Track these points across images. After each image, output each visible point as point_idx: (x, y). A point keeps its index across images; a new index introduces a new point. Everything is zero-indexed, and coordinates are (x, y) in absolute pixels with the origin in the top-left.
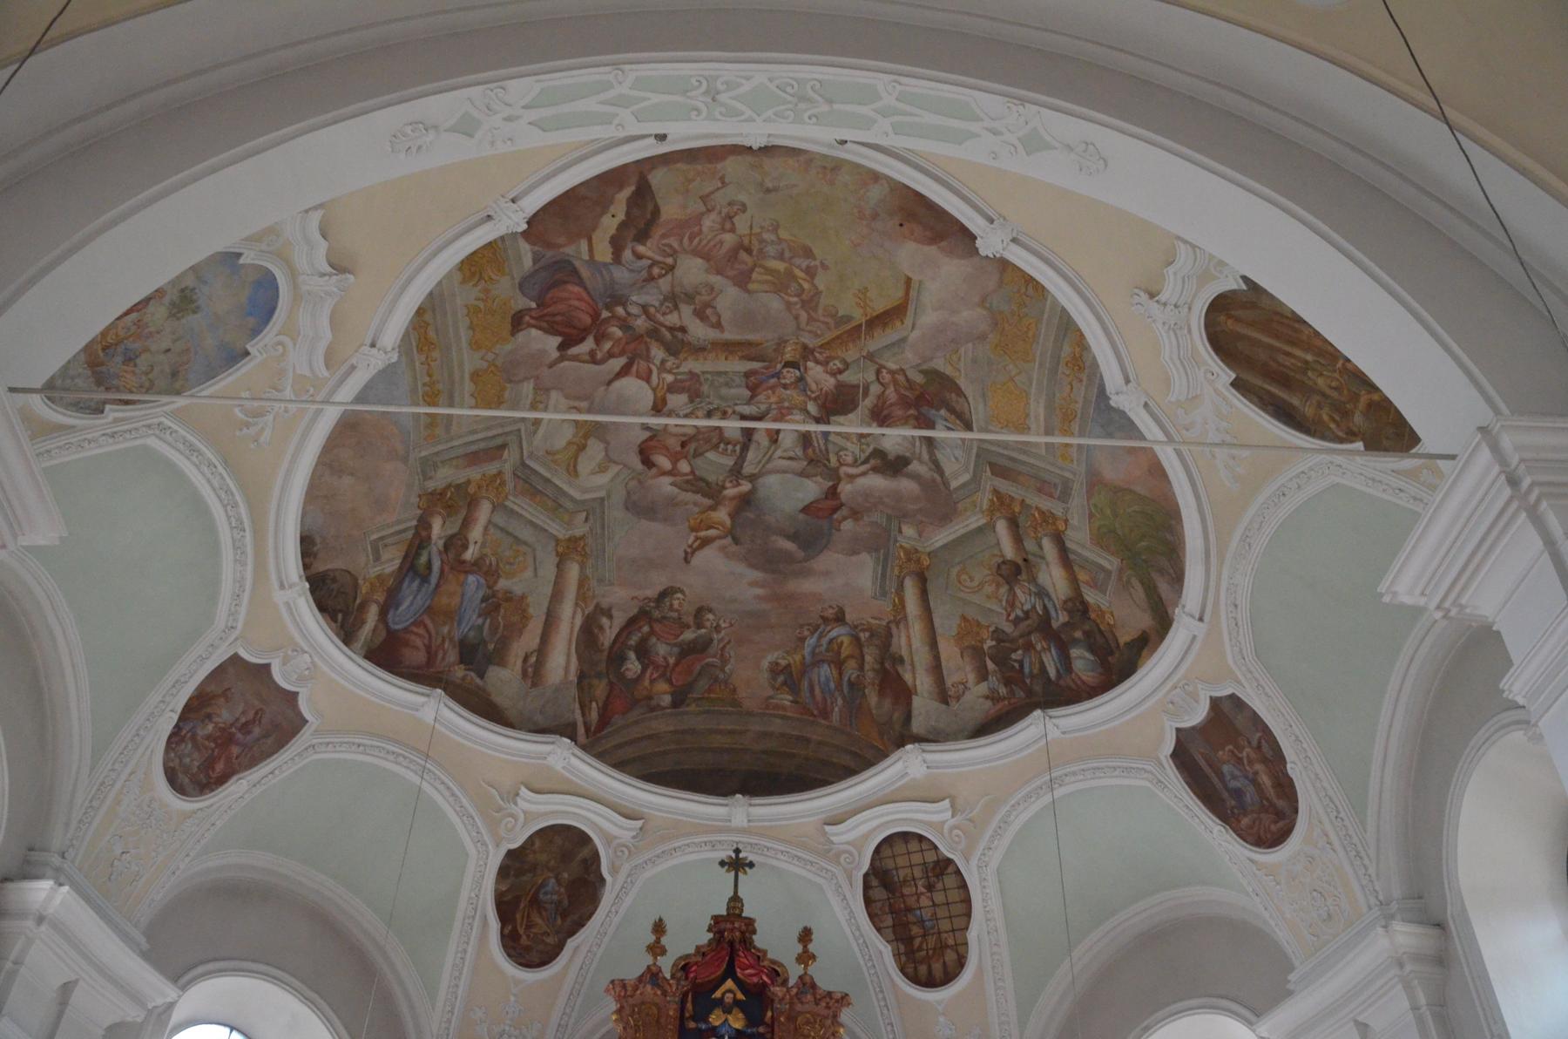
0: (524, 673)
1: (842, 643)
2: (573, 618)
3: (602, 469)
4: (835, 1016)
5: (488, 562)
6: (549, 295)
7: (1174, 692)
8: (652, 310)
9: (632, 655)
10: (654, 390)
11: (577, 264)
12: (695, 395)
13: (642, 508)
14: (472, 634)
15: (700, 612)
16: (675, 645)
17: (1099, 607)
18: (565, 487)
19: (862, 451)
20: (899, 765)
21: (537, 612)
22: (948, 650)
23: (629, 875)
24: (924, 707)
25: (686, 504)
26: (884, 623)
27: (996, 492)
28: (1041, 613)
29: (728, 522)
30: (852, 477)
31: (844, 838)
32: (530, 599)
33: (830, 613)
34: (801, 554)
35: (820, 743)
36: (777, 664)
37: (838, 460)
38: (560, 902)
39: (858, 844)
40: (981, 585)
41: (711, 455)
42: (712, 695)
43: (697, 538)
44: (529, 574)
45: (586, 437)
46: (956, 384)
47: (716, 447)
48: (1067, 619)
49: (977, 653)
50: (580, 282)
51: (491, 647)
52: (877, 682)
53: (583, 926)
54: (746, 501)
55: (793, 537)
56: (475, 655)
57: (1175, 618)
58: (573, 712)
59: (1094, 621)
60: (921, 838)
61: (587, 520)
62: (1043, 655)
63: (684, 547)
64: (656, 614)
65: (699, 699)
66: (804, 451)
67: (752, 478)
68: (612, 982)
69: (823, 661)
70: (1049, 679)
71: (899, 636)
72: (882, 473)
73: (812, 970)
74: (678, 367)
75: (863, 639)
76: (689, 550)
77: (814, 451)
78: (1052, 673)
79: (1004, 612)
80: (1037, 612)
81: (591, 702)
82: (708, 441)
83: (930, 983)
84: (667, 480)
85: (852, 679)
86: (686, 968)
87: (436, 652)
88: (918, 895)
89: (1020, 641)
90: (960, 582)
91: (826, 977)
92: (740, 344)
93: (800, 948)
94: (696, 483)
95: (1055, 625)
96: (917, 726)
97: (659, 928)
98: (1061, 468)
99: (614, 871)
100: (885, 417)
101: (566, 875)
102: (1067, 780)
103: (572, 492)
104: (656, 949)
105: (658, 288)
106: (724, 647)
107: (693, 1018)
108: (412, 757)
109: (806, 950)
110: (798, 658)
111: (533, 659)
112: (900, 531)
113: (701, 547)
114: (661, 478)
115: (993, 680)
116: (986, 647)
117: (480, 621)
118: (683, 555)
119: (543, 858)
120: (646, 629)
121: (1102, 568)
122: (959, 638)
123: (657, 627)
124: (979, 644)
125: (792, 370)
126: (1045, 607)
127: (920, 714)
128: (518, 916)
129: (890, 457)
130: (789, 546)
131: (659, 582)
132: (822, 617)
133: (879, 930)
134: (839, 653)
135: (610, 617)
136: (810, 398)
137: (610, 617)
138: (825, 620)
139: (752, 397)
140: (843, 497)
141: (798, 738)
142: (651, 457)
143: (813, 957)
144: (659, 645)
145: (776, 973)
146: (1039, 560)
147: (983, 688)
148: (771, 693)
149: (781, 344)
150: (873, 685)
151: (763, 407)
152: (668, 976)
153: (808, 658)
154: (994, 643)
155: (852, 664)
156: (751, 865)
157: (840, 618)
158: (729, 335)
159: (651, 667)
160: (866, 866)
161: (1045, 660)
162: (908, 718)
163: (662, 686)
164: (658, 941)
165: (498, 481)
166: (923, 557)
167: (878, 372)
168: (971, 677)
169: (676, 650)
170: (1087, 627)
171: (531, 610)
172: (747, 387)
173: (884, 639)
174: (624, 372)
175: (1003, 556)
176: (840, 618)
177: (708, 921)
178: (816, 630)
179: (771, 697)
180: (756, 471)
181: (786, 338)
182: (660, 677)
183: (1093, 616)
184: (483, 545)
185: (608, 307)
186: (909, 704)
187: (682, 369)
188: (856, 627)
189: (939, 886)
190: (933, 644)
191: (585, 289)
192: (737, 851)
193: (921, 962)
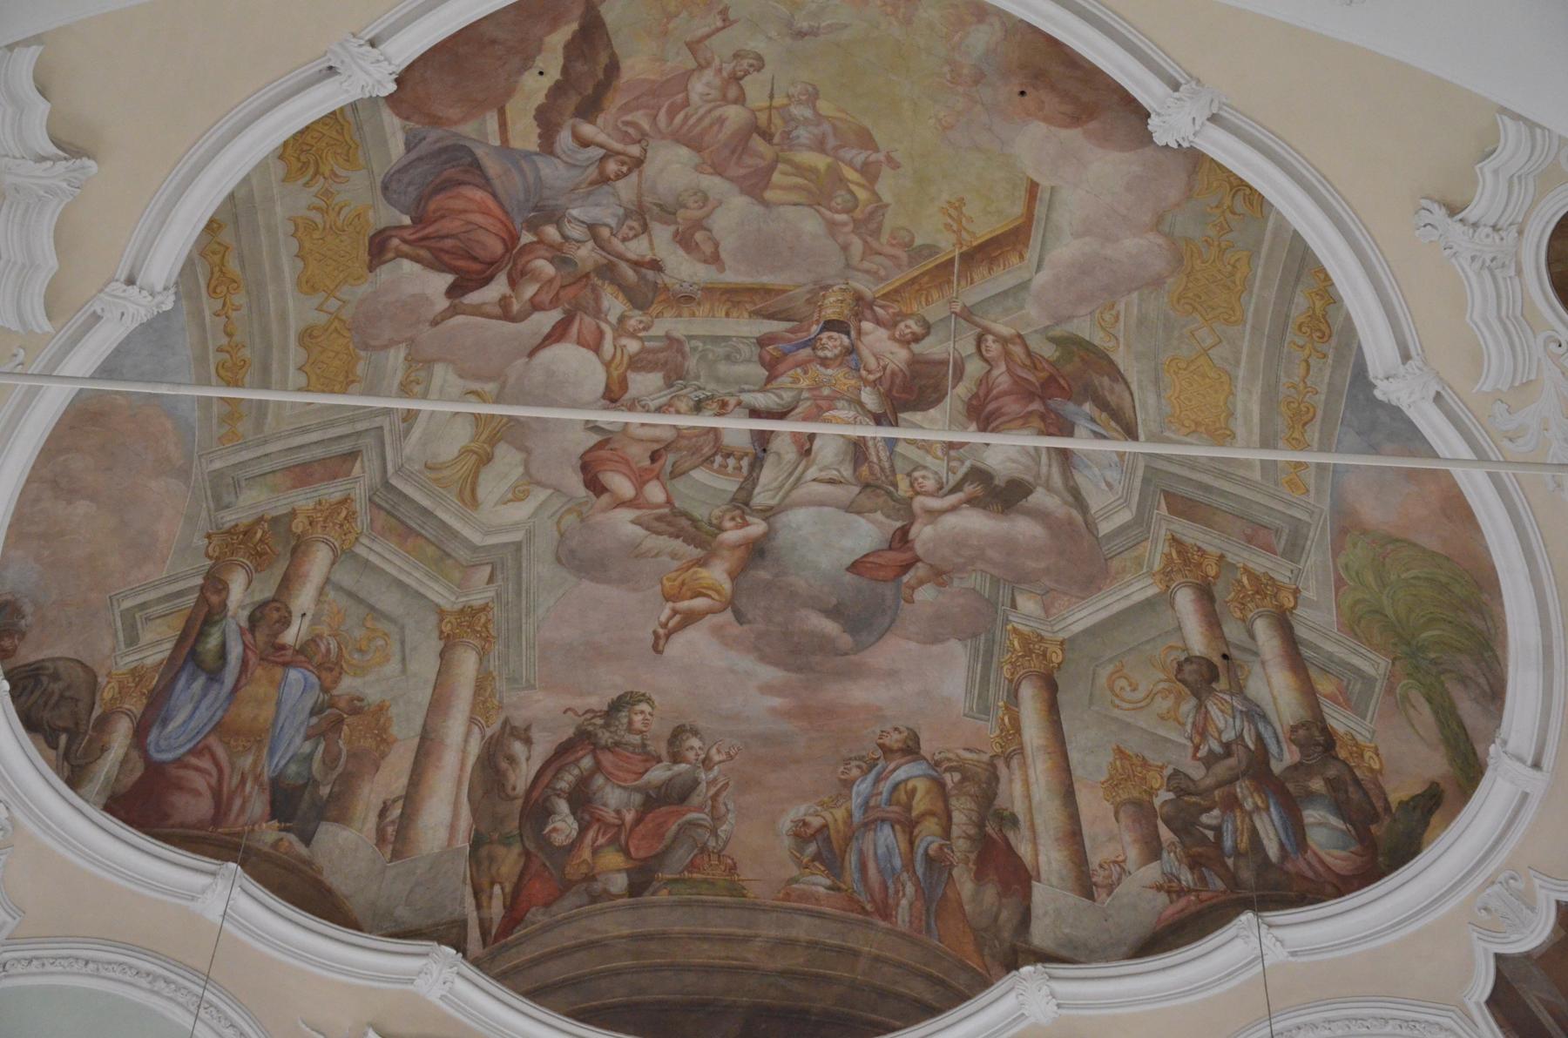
1: (914, 791)
2: (466, 741)
3: (518, 495)
5: (323, 648)
6: (432, 206)
7: (1488, 891)
8: (605, 232)
9: (563, 806)
10: (607, 365)
11: (480, 152)
12: (675, 375)
14: (293, 768)
15: (678, 734)
16: (637, 789)
17: (1354, 738)
18: (456, 525)
19: (951, 470)
20: (1009, 1002)
21: (405, 730)
22: (1093, 806)
25: (657, 555)
26: (985, 758)
27: (1175, 541)
28: (1252, 747)
29: (727, 586)
30: (933, 514)
32: (393, 711)
33: (893, 740)
34: (846, 640)
35: (877, 959)
36: (805, 824)
37: (912, 485)
40: (1151, 696)
41: (700, 475)
42: (695, 875)
43: (675, 612)
44: (393, 667)
45: (493, 441)
46: (1112, 363)
47: (709, 460)
48: (1297, 757)
49: (1143, 812)
50: (486, 183)
51: (325, 791)
52: (973, 856)
54: (757, 551)
55: (834, 613)
57: (1491, 762)
58: (462, 902)
59: (1344, 762)
61: (491, 580)
62: (1256, 818)
63: (654, 625)
64: (605, 737)
65: (676, 881)
66: (855, 470)
67: (768, 513)
69: (883, 820)
70: (1266, 857)
71: (1011, 781)
72: (984, 508)
74: (646, 329)
75: (950, 784)
76: (661, 631)
77: (871, 469)
78: (1273, 850)
79: (1189, 744)
80: (1247, 747)
81: (492, 884)
82: (695, 450)
84: (626, 515)
85: (931, 852)
87: (231, 799)
89: (1216, 792)
90: (1112, 690)
92: (751, 291)
94: (675, 522)
95: (1277, 767)
96: (1040, 935)
98: (1290, 504)
100: (992, 413)
103: (466, 532)
105: (616, 194)
106: (717, 794)
108: (180, 980)
110: (840, 814)
111: (396, 812)
112: (1014, 606)
113: (682, 626)
114: (617, 510)
115: (1171, 861)
116: (1157, 802)
117: (307, 747)
118: (650, 639)
120: (587, 763)
121: (1358, 672)
123: (607, 759)
124: (1146, 797)
125: (835, 335)
126: (1259, 738)
127: (1046, 913)
129: (996, 482)
130: (830, 627)
131: (608, 684)
132: (882, 746)
134: (909, 808)
135: (528, 741)
136: (866, 382)
137: (528, 741)
138: (887, 751)
139: (770, 380)
140: (919, 549)
141: (841, 950)
142: (601, 476)
144: (608, 789)
146: (1253, 658)
147: (1152, 872)
150: (967, 862)
151: (788, 396)
153: (858, 817)
154: (1171, 796)
155: (930, 826)
157: (911, 749)
158: (731, 277)
159: (596, 827)
161: (1259, 825)
163: (613, 859)
165: (343, 514)
166: (1051, 648)
167: (980, 341)
168: (1133, 853)
169: (637, 798)
170: (1332, 772)
171: (394, 730)
172: (763, 364)
173: (986, 787)
174: (557, 334)
175: (1186, 649)
176: (911, 749)
178: (870, 770)
179: (794, 880)
180: (772, 502)
181: (830, 282)
182: (611, 842)
183: (1342, 754)
184: (316, 620)
185: (533, 226)
187: (652, 332)
188: (937, 764)
190: (1068, 795)
191: (494, 195)
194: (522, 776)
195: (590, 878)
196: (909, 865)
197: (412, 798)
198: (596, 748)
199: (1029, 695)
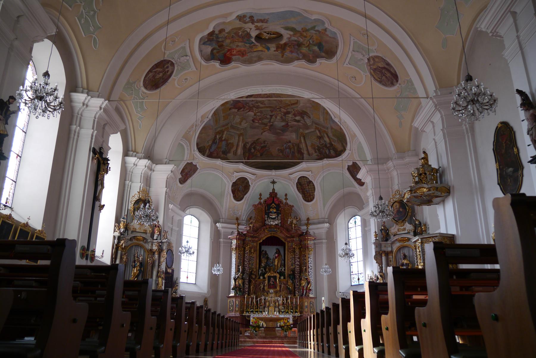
0: (234, 154)
3: (245, 123)
4: (291, 209)
9: (253, 149)
10: (254, 113)
13: (252, 127)
15: (264, 142)
21: (235, 144)
22: (310, 148)
23: (255, 184)
29: (268, 128)
31: (293, 177)
38: (243, 190)
39: (295, 178)
41: (265, 120)
49: (314, 149)
51: (228, 151)
53: (247, 193)
54: (271, 125)
55: (280, 130)
56: (225, 153)
67: (272, 122)
68: (253, 205)
73: (287, 201)
78: (328, 154)
83: (308, 201)
86: (265, 202)
88: (306, 187)
91: (290, 202)
94: (263, 123)
99: (252, 184)
101: (243, 185)
102: (331, 170)
104: (260, 199)
107: (267, 210)
109: (286, 198)
110: (283, 148)
111: (235, 151)
112: (300, 130)
128: (236, 193)
130: (280, 131)
131: (257, 137)
134: (290, 147)
135: (248, 144)
137: (248, 144)
138: (287, 142)
143: (287, 199)
145: (281, 202)
147: (316, 154)
152: (263, 203)
153: (285, 148)
157: (290, 142)
158: (267, 106)
163: (258, 153)
164: (260, 197)
168: (314, 152)
173: (298, 146)
174: (249, 111)
176: (290, 142)
177: (269, 193)
186: (303, 155)
189: (310, 185)
190: (307, 147)
194: (248, 146)
196: (290, 152)
199: (302, 137)
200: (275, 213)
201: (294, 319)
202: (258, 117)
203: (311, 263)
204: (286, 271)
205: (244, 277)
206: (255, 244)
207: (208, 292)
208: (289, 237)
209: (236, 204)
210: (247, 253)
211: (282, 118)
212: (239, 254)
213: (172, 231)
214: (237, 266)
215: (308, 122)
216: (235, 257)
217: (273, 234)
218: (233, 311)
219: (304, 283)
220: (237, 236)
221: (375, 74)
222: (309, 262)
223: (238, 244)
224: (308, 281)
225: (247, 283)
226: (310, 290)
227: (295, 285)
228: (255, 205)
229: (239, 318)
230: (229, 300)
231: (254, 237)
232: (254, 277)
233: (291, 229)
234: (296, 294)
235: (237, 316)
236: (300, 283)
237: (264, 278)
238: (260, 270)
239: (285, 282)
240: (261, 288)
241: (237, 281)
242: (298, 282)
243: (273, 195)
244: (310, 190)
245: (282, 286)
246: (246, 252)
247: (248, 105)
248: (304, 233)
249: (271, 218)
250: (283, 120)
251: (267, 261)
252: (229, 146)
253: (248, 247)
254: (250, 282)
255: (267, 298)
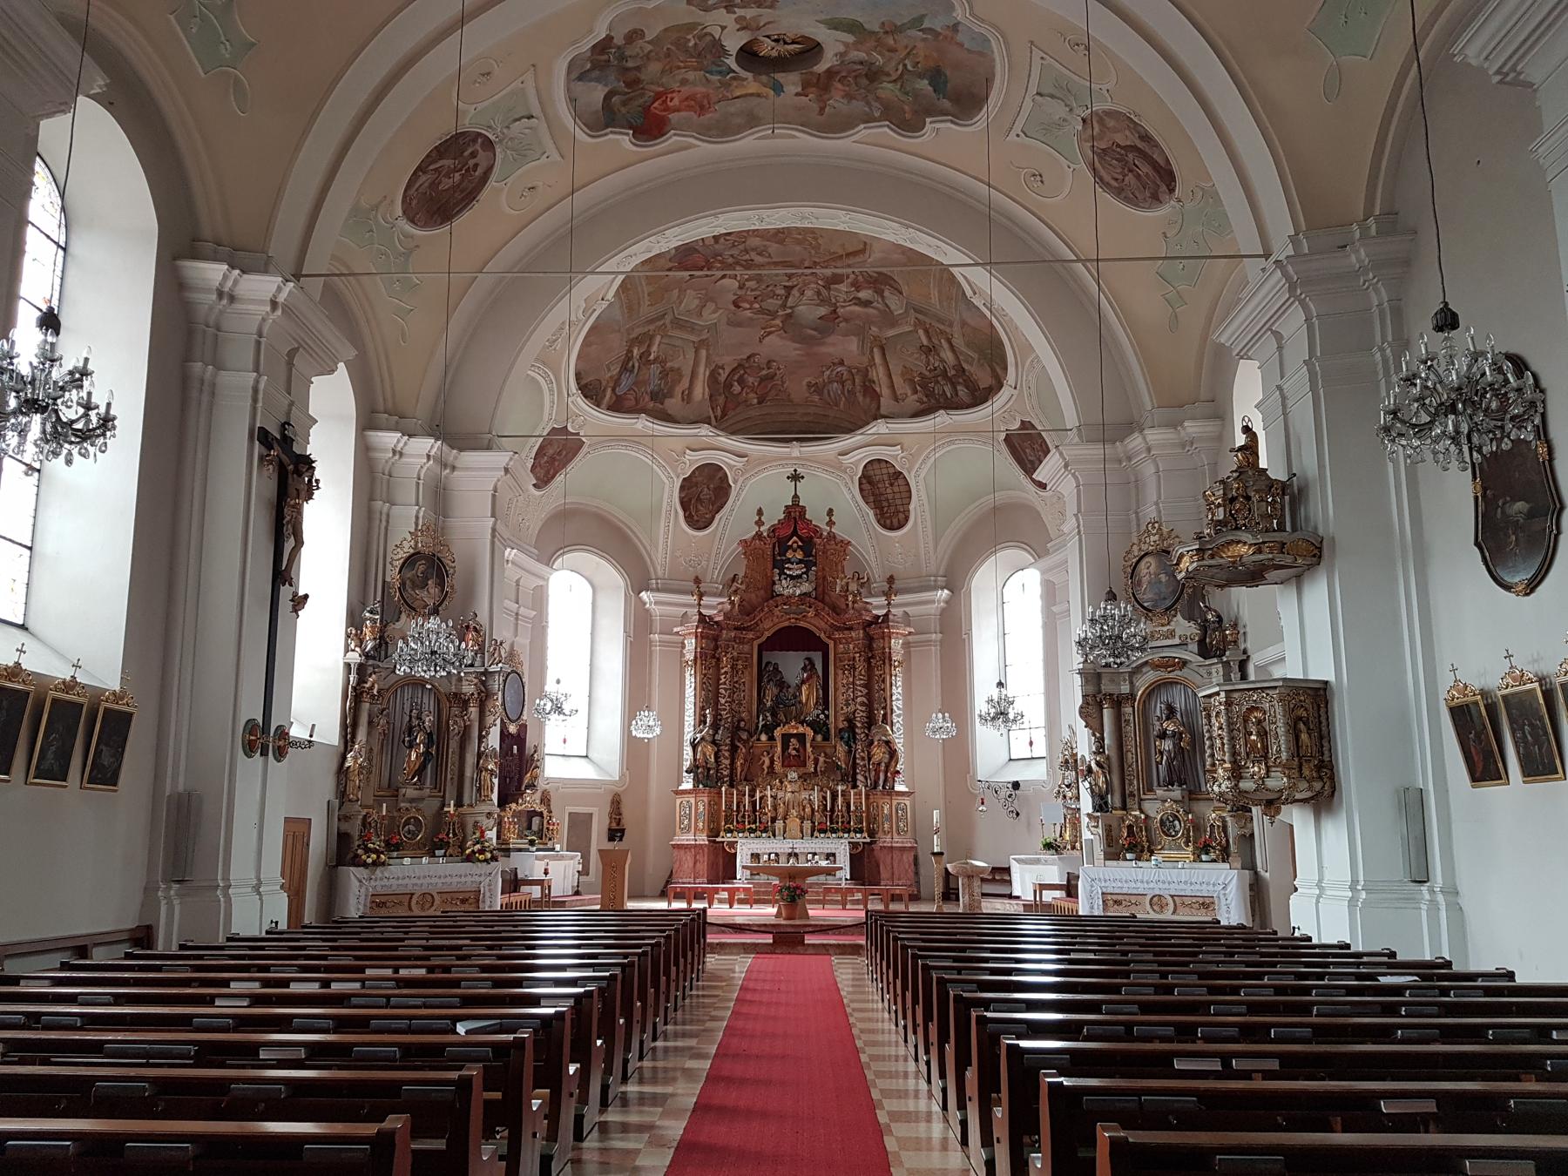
0: (683, 400)
3: (714, 312)
9: (736, 383)
22: (897, 380)
24: (886, 402)
39: (856, 464)
49: (911, 381)
54: (790, 316)
55: (815, 330)
60: (887, 462)
64: (747, 365)
67: (791, 308)
78: (949, 395)
83: (892, 528)
93: (828, 519)
96: (883, 411)
97: (760, 512)
99: (735, 482)
104: (759, 523)
107: (779, 555)
109: (831, 520)
119: (700, 479)
122: (903, 375)
123: (748, 371)
131: (747, 352)
133: (867, 503)
138: (834, 364)
147: (915, 397)
148: (808, 395)
149: (802, 261)
156: (803, 477)
157: (842, 363)
158: (774, 260)
160: (860, 474)
162: (879, 408)
163: (752, 395)
168: (909, 392)
173: (865, 373)
176: (842, 363)
190: (890, 376)
192: (795, 471)
193: (887, 518)
194: (722, 378)
195: (746, 401)
196: (843, 393)
197: (691, 388)
198: (744, 368)
200: (800, 562)
201: (854, 852)
202: (749, 293)
203: (898, 699)
204: (832, 719)
205: (718, 737)
206: (746, 648)
207: (622, 776)
208: (838, 629)
209: (694, 537)
210: (726, 673)
211: (819, 293)
212: (705, 675)
213: (517, 619)
214: (698, 710)
215: (895, 304)
216: (693, 685)
217: (796, 619)
218: (689, 831)
219: (879, 754)
220: (697, 627)
221: (1104, 168)
222: (894, 698)
223: (702, 648)
224: (890, 747)
225: (727, 754)
226: (898, 772)
227: (855, 758)
228: (745, 541)
229: (706, 849)
230: (678, 802)
231: (744, 629)
232: (744, 736)
233: (844, 607)
234: (858, 783)
235: (702, 843)
236: (869, 753)
237: (772, 738)
238: (761, 718)
239: (828, 751)
240: (765, 767)
241: (700, 749)
242: (863, 751)
243: (795, 513)
244: (897, 496)
245: (821, 759)
246: (723, 671)
247: (720, 258)
248: (879, 617)
249: (792, 578)
250: (823, 301)
251: (781, 691)
252: (670, 375)
253: (729, 655)
254: (734, 749)
255: (780, 794)
